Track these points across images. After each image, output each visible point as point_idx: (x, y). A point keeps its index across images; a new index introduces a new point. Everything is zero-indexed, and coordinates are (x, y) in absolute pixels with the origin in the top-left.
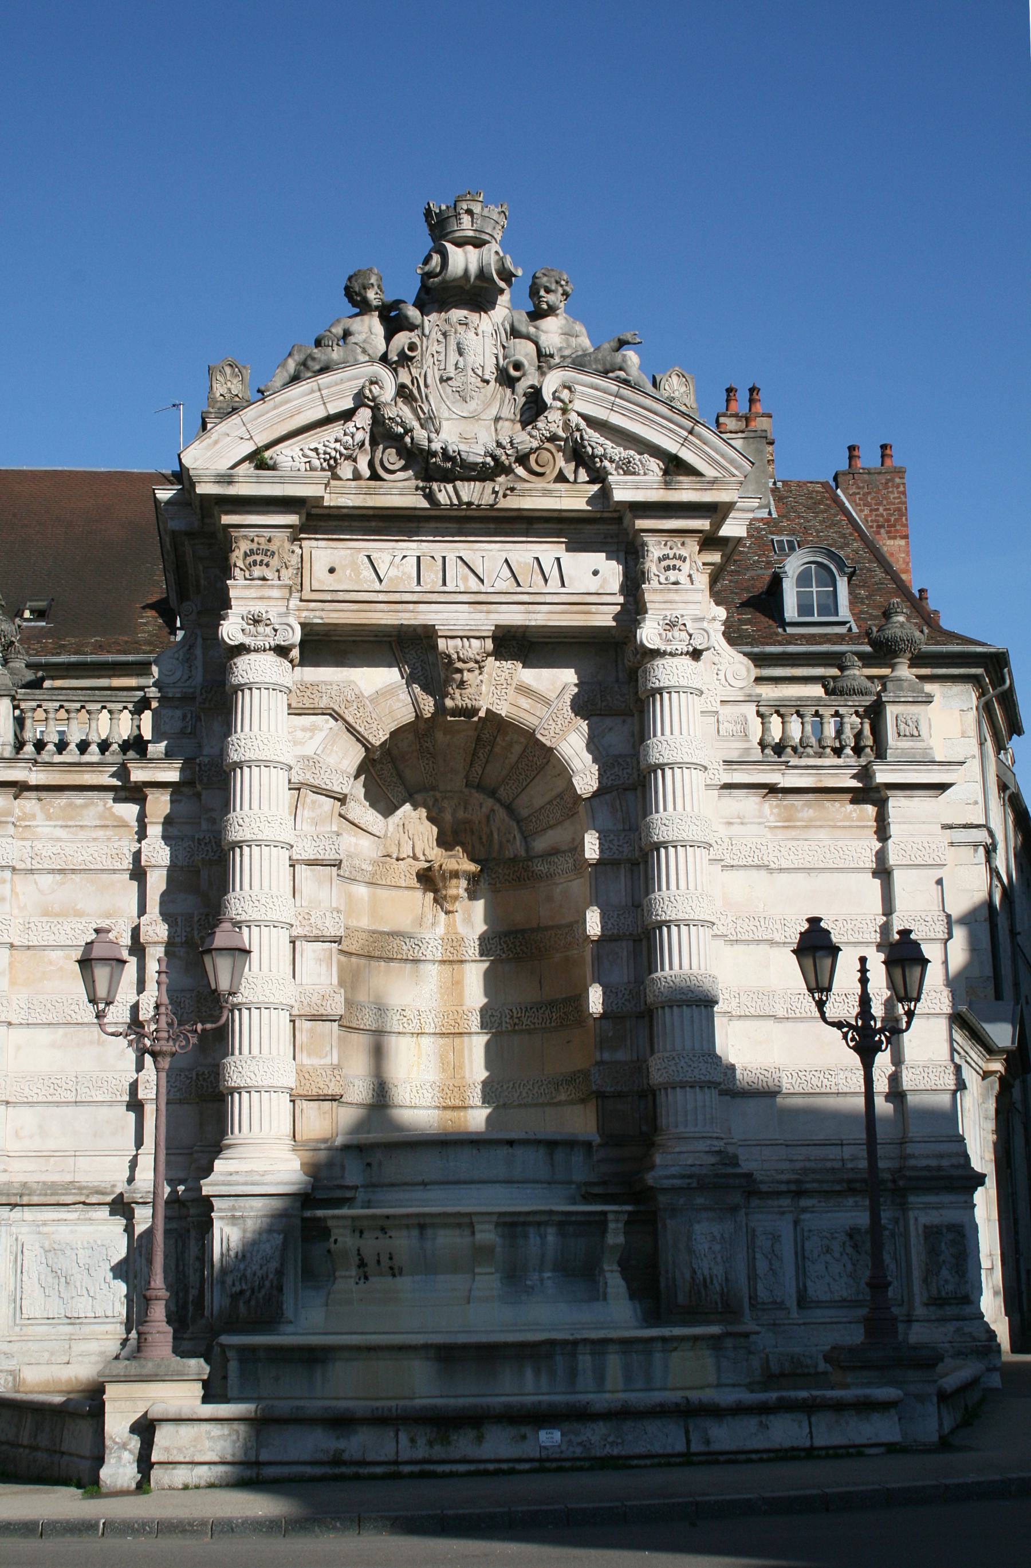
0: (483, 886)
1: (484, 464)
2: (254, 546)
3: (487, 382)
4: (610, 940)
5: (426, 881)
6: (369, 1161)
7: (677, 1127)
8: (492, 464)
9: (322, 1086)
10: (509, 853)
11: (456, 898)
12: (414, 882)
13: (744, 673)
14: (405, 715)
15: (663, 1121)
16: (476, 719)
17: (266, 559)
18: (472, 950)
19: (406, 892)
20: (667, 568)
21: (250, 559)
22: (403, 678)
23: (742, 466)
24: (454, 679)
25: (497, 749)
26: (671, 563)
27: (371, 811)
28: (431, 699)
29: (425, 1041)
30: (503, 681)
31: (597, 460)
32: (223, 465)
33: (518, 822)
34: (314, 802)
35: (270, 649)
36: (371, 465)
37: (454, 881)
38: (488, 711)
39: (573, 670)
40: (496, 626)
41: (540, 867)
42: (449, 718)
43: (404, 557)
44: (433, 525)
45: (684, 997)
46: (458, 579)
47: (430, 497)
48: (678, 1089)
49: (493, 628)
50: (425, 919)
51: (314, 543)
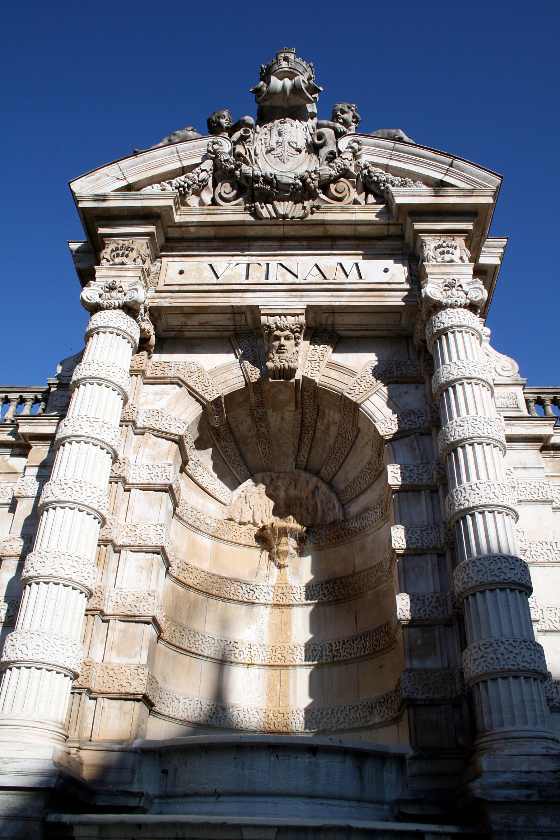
0: (309, 545)
1: (294, 185)
3: (299, 151)
4: (416, 555)
5: (263, 541)
6: (166, 768)
7: (502, 725)
8: (301, 184)
9: (124, 684)
10: (330, 519)
11: (286, 553)
12: (253, 542)
13: (510, 367)
14: (238, 383)
15: (484, 721)
16: (293, 380)
18: (300, 596)
19: (246, 550)
20: (442, 253)
21: (115, 253)
22: (237, 358)
23: (494, 180)
24: (274, 346)
25: (318, 435)
26: (445, 250)
27: (218, 481)
28: (257, 370)
29: (255, 671)
30: (316, 358)
31: (382, 184)
33: (337, 495)
34: (155, 444)
35: (119, 308)
37: (284, 540)
39: (374, 354)
40: (308, 306)
41: (355, 525)
42: (271, 380)
43: (238, 264)
44: (259, 243)
45: (497, 579)
47: (255, 214)
48: (500, 680)
49: (306, 307)
50: (261, 571)
51: (171, 259)
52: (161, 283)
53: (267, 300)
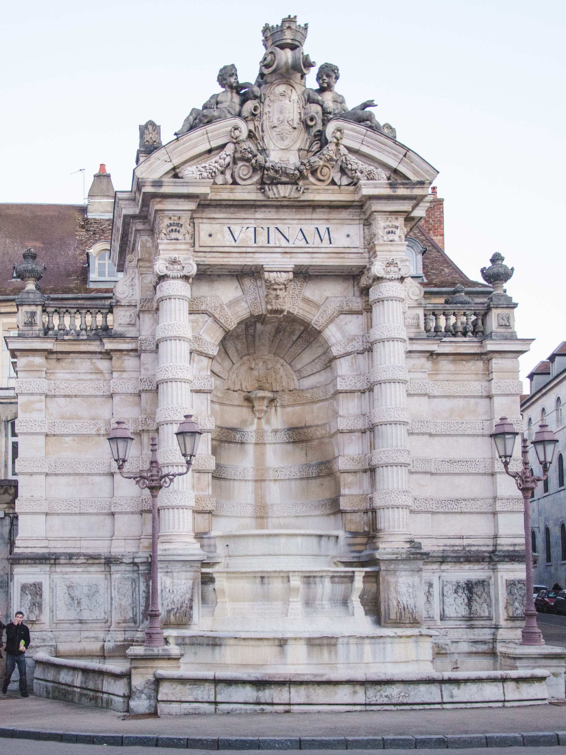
2: (172, 222)
8: (298, 174)
17: (178, 229)
21: (170, 229)
32: (156, 176)
36: (232, 176)
38: (288, 312)
40: (295, 265)
43: (248, 228)
46: (276, 239)
52: (197, 245)
53: (268, 260)
